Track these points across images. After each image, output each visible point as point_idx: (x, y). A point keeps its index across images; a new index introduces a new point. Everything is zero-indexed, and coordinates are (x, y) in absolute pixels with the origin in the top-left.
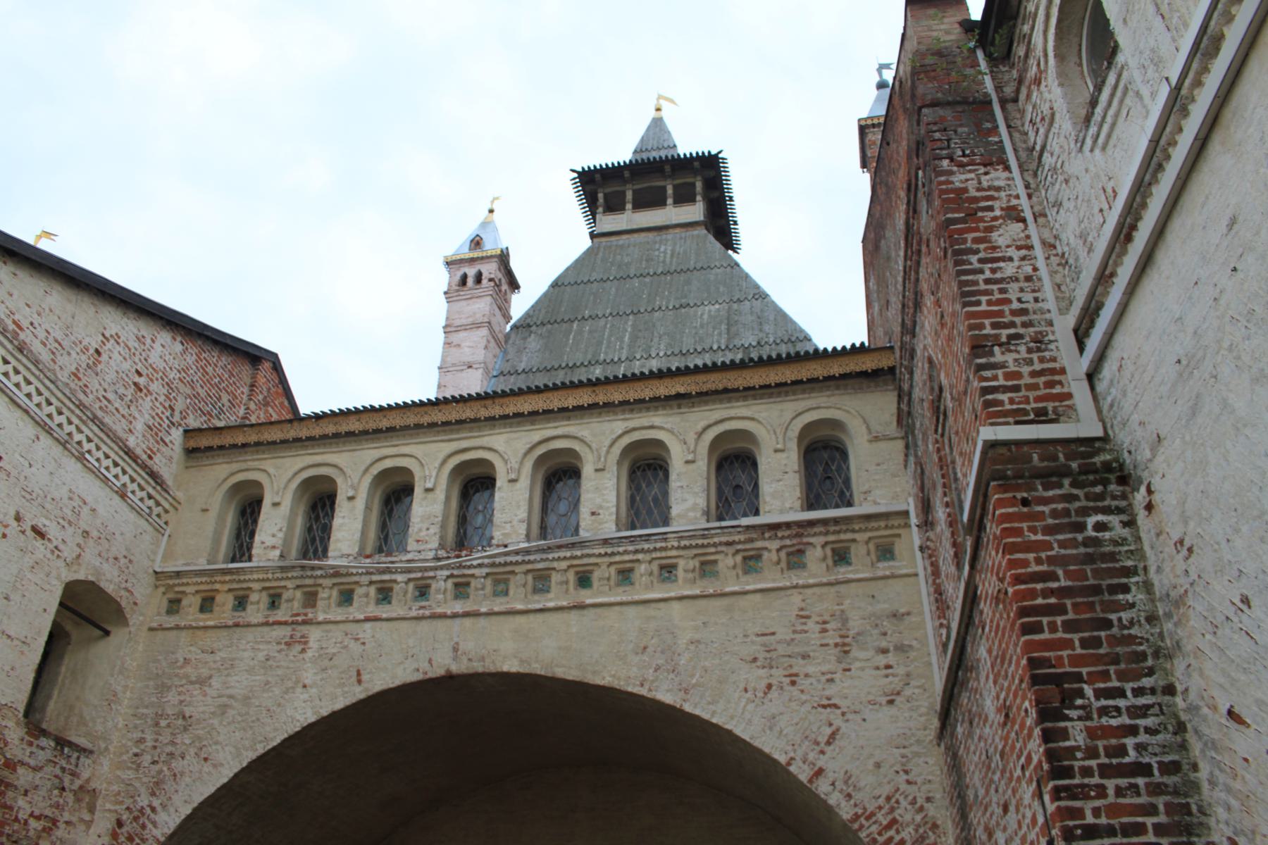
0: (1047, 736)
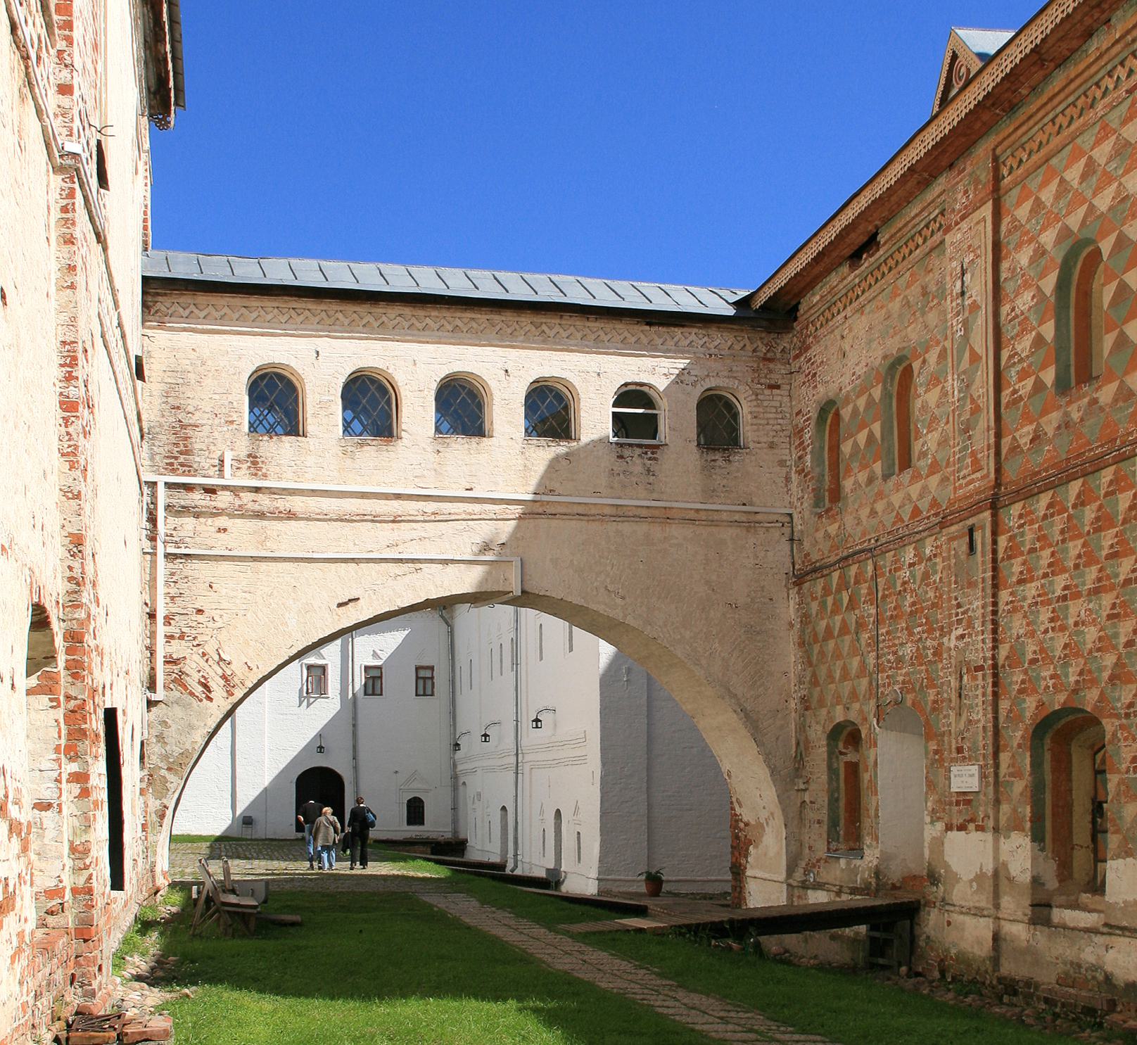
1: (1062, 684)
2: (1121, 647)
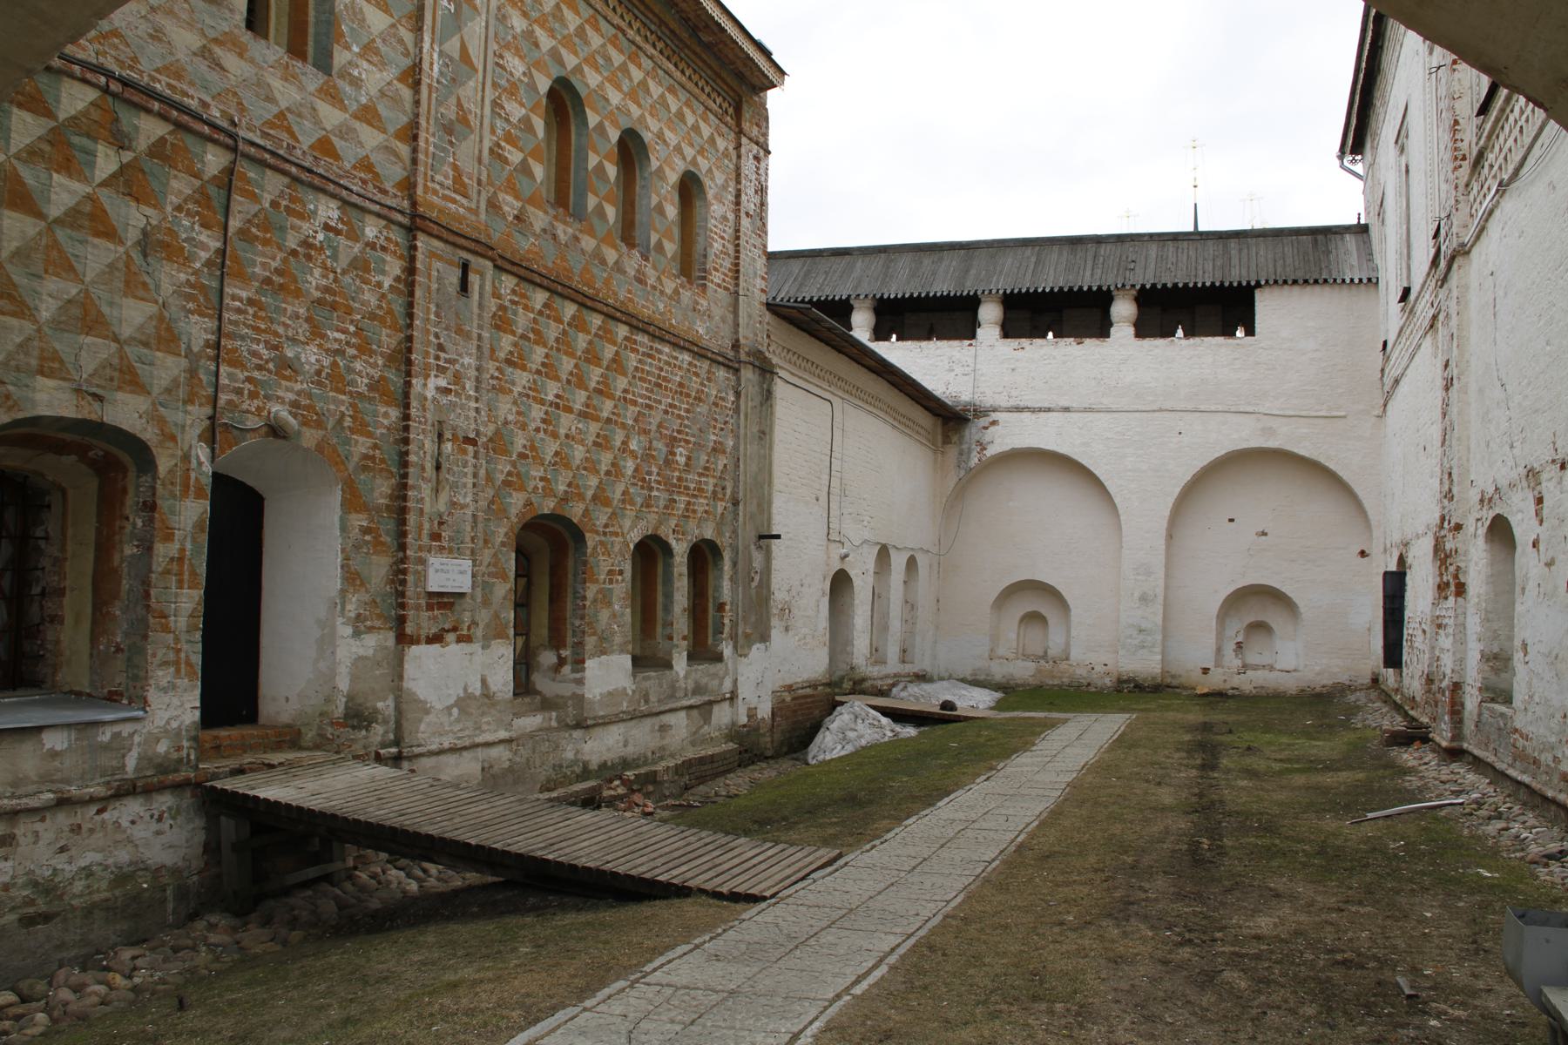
1: (552, 490)
2: (602, 473)
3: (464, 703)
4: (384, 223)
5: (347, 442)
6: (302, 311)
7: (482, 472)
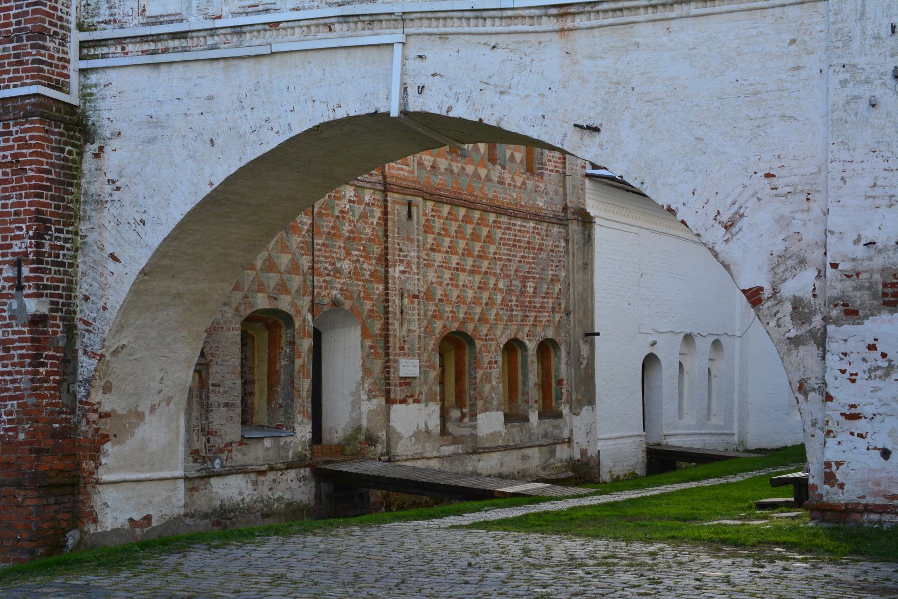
0: (39, 245)
1: (456, 317)
3: (417, 435)
4: (372, 191)
5: (362, 304)
6: (342, 244)
7: (422, 312)
